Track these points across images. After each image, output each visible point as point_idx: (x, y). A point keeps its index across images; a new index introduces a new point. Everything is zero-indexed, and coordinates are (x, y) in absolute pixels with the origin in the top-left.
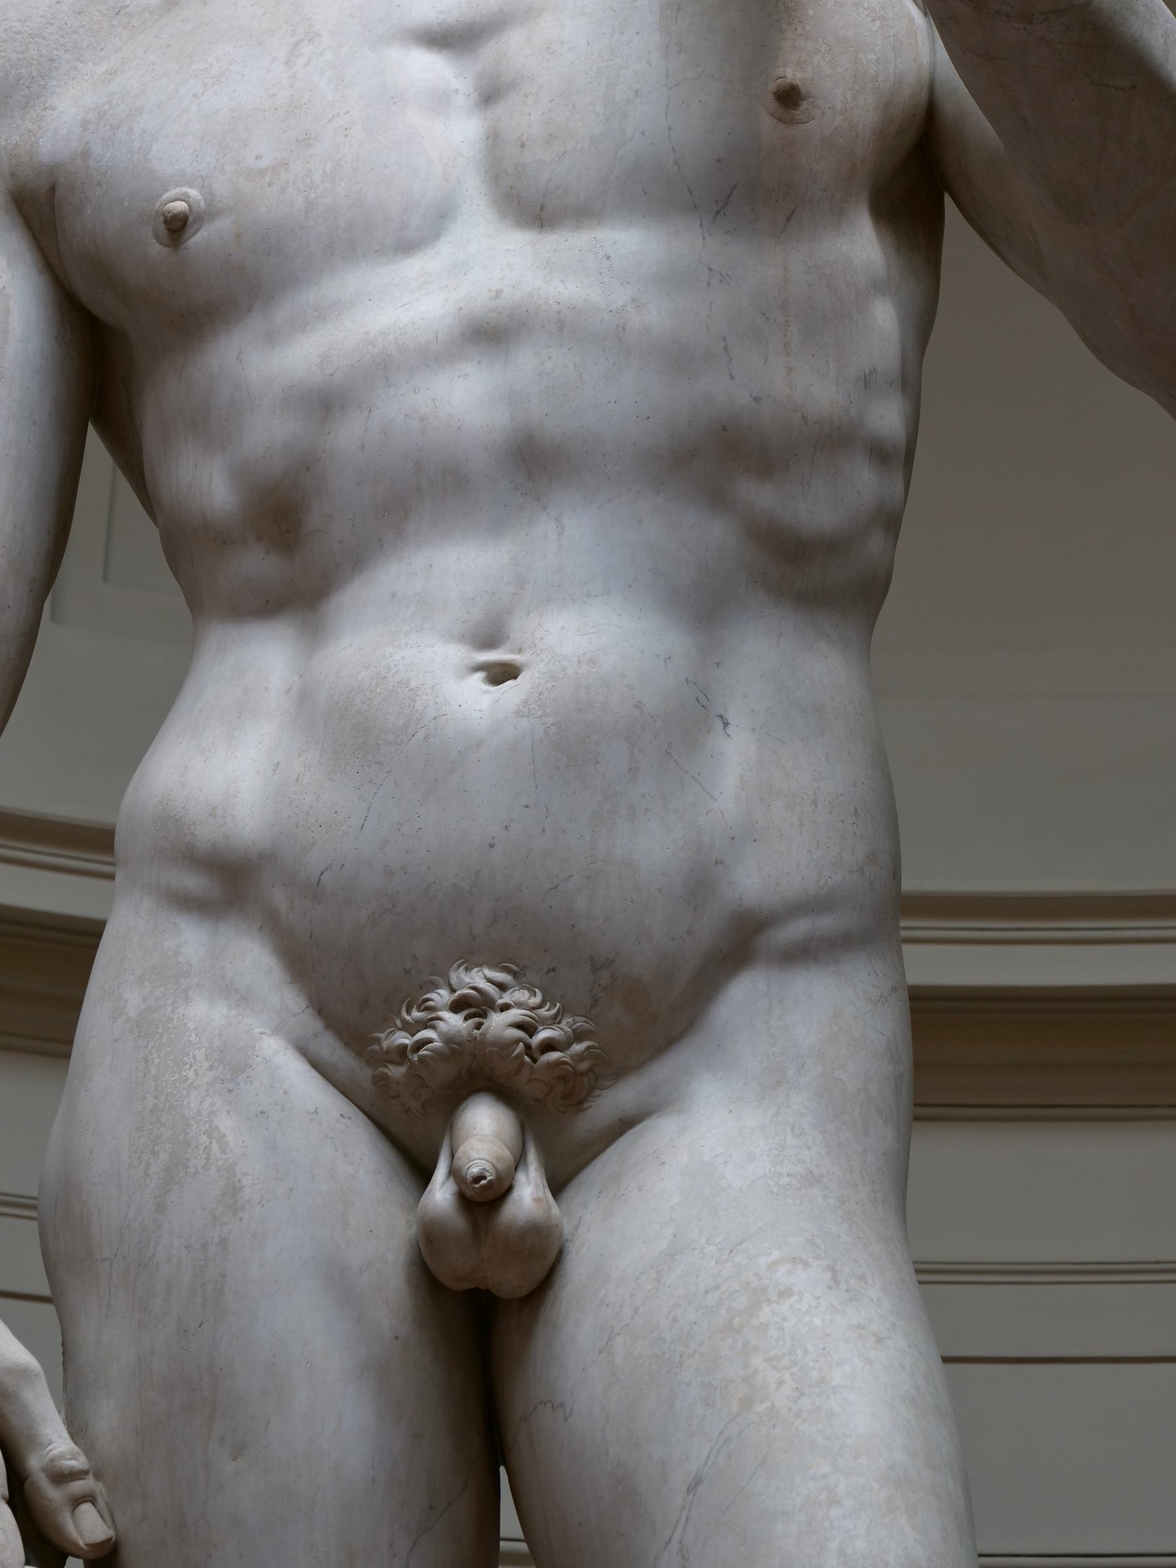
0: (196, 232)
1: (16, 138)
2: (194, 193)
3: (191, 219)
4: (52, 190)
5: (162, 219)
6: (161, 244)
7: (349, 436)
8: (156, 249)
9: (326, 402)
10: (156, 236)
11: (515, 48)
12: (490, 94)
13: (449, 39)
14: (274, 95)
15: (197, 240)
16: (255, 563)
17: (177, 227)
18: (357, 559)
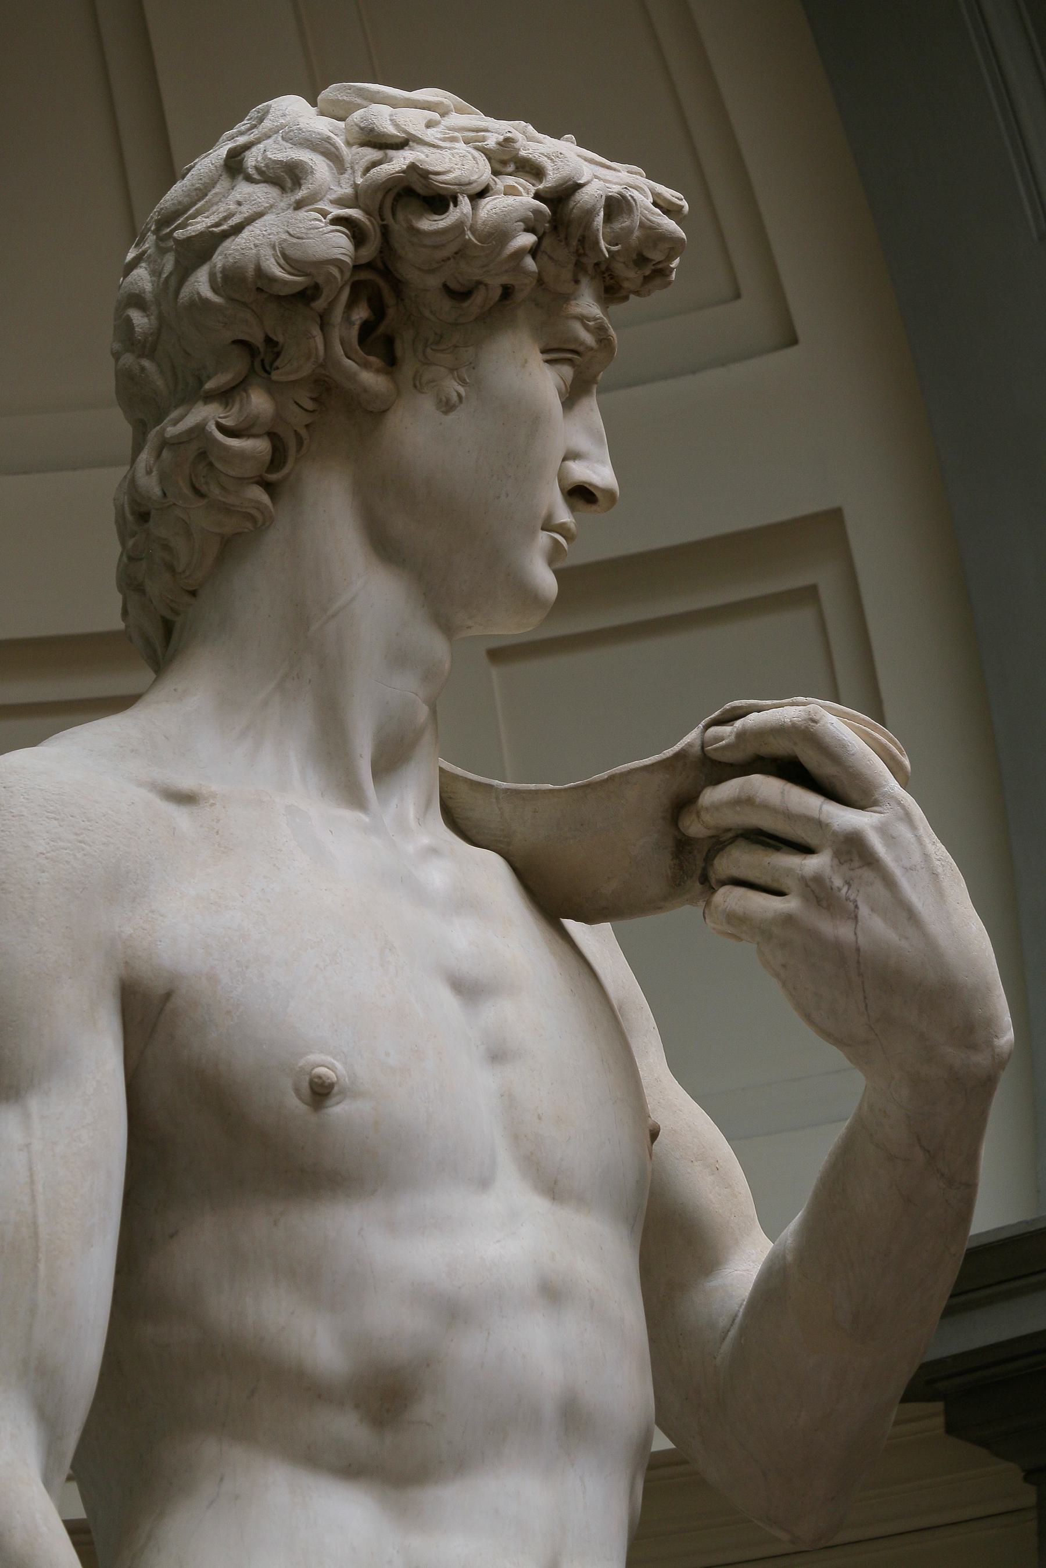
0: (338, 1103)
1: (128, 930)
2: (339, 1066)
3: (336, 1089)
4: (168, 996)
5: (307, 1078)
6: (300, 1099)
7: (468, 1349)
8: (295, 1104)
9: (453, 1311)
10: (297, 1091)
11: (503, 1013)
12: (498, 1055)
13: (469, 989)
14: (383, 996)
15: (338, 1110)
16: (347, 1427)
17: (320, 1092)
18: (458, 1464)
